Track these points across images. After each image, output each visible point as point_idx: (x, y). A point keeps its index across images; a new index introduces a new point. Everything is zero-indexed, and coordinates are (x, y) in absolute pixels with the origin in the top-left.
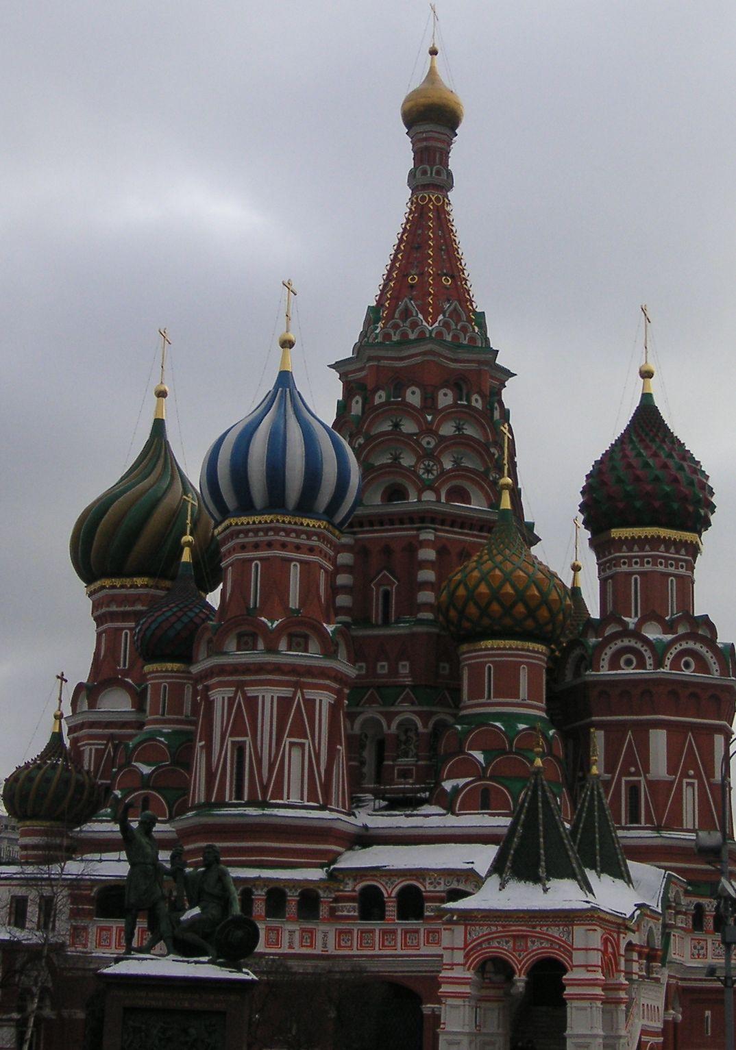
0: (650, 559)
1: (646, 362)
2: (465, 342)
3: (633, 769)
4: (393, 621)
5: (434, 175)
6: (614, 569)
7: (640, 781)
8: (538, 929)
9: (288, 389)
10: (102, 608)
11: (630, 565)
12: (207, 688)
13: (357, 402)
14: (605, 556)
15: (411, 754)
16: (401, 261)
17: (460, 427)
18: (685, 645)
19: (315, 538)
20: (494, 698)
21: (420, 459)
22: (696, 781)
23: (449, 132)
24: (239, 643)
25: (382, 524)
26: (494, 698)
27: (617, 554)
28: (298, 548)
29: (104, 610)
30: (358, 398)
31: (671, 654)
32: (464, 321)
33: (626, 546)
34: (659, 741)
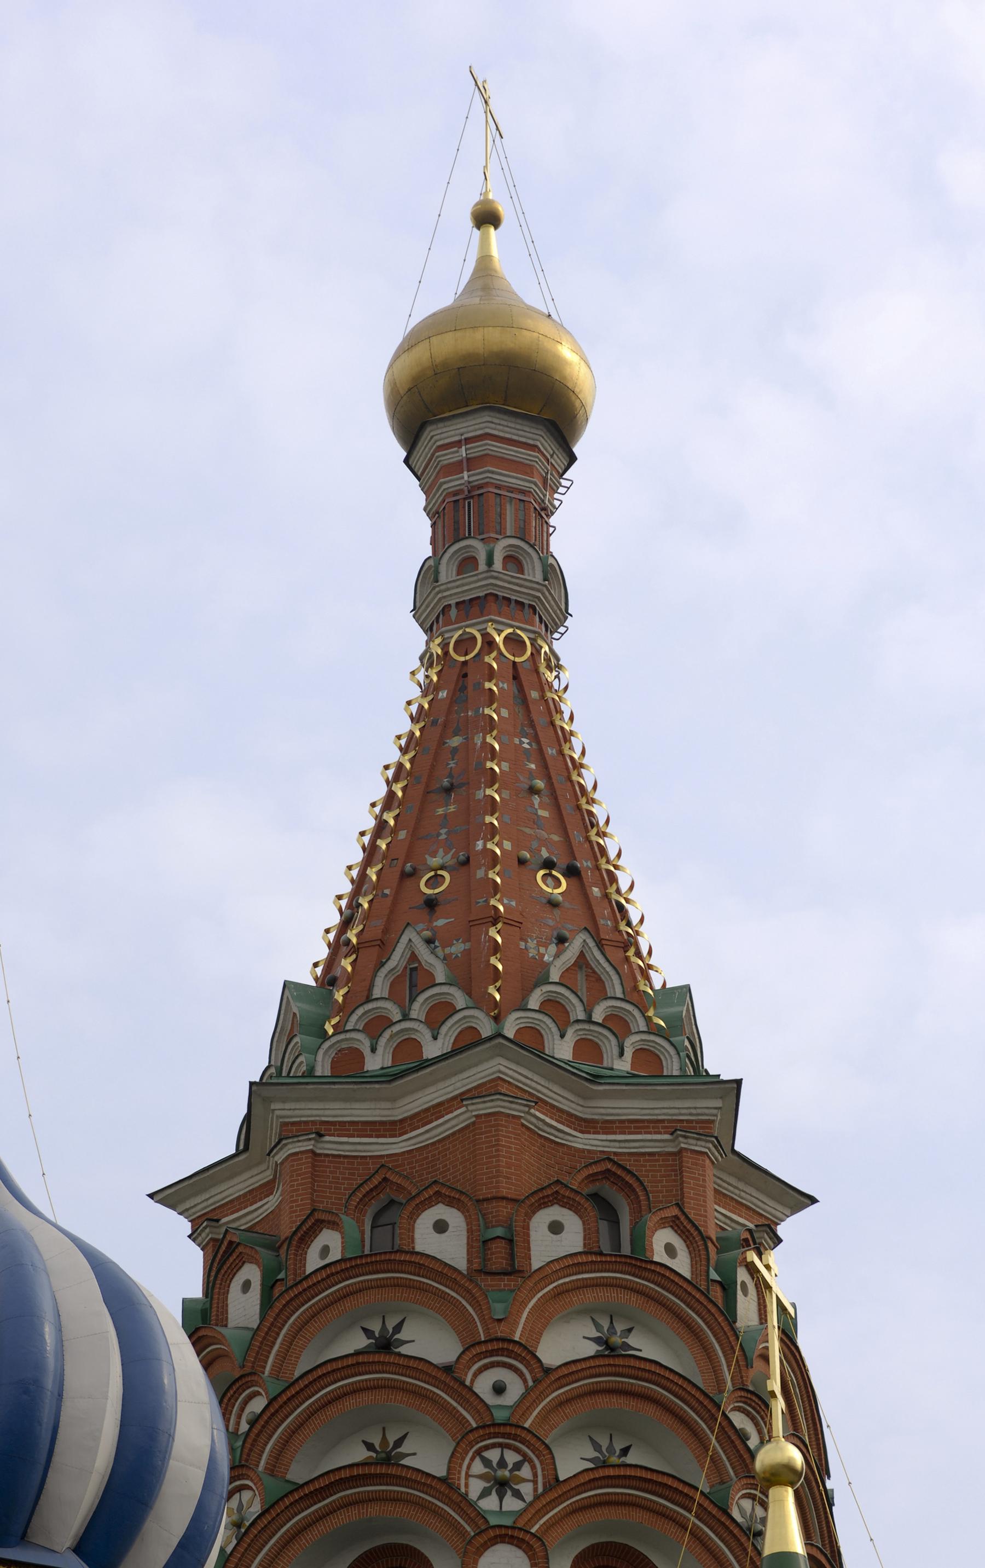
2: (624, 1065)
5: (498, 565)
13: (246, 1286)
16: (394, 831)
17: (616, 1340)
23: (547, 444)
30: (251, 1273)
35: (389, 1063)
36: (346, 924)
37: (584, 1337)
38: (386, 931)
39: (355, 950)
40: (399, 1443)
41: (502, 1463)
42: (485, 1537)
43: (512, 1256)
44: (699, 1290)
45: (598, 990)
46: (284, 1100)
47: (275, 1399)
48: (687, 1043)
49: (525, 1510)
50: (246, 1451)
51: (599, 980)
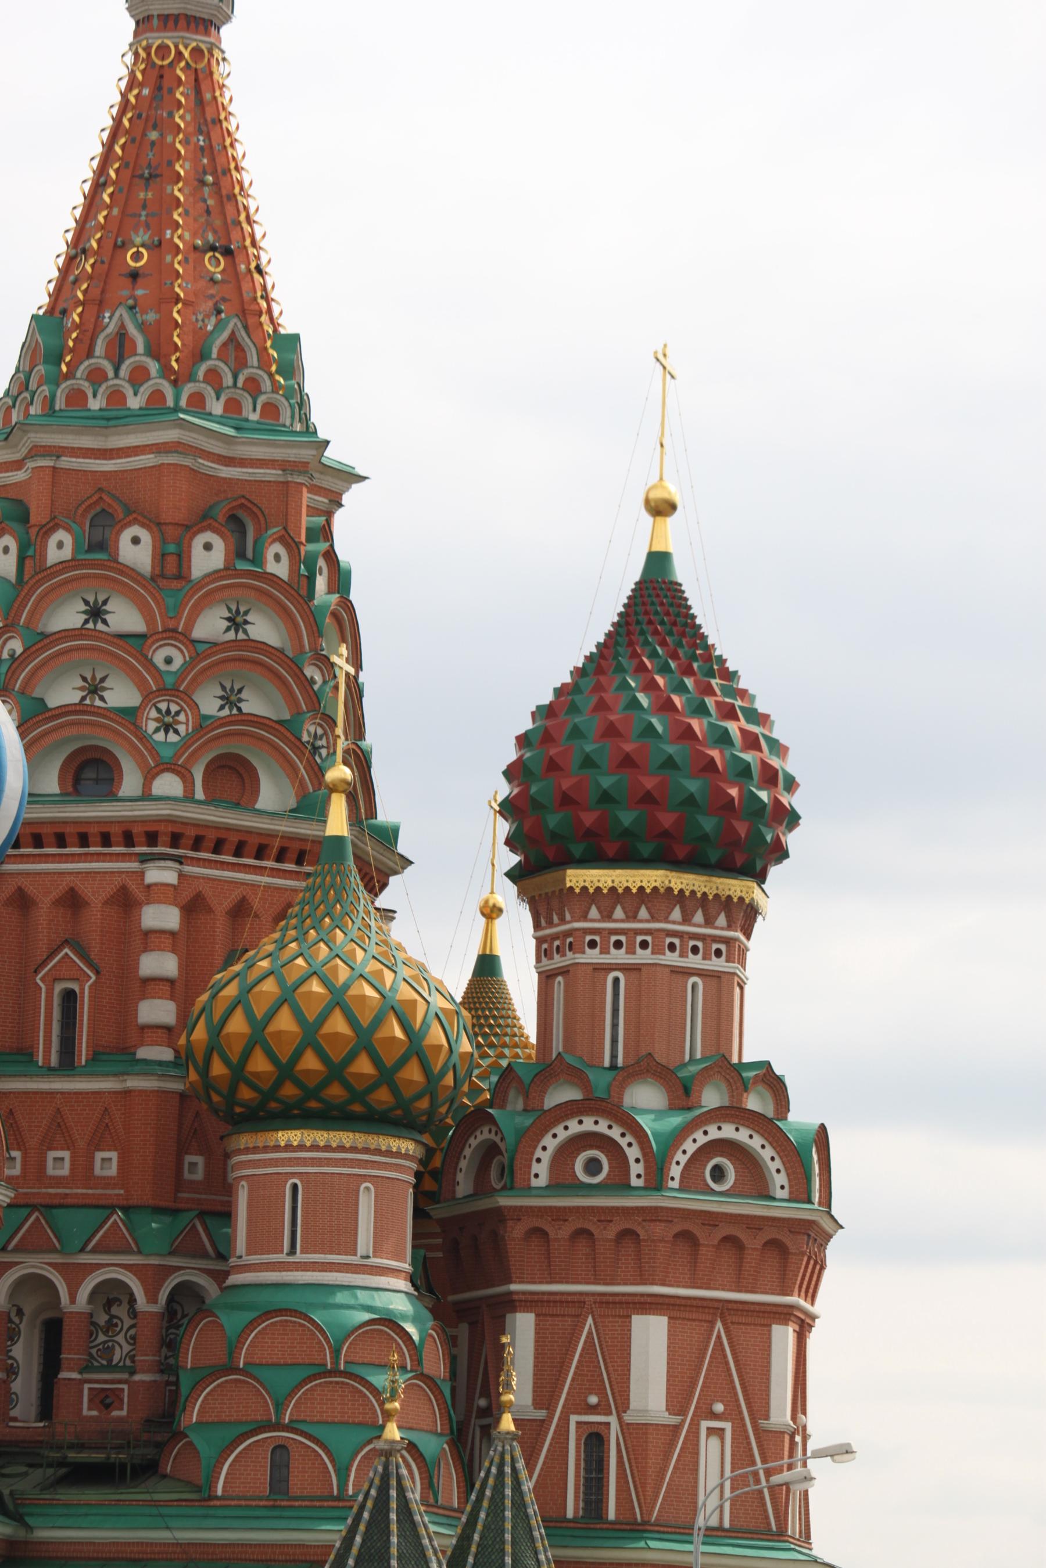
0: (649, 939)
1: (661, 479)
2: (254, 417)
3: (593, 1400)
6: (569, 954)
7: (608, 1424)
11: (605, 951)
14: (550, 924)
15: (116, 1358)
16: (109, 207)
17: (239, 619)
18: (714, 1134)
20: (302, 1252)
21: (148, 697)
22: (727, 1426)
25: (61, 841)
26: (302, 1252)
31: (684, 1152)
32: (253, 367)
33: (598, 908)
35: (104, 405)
36: (70, 260)
37: (221, 618)
38: (103, 292)
39: (83, 304)
40: (103, 680)
41: (168, 712)
42: (158, 769)
43: (179, 566)
44: (293, 589)
45: (241, 363)
46: (36, 432)
47: (28, 648)
48: (296, 386)
49: (180, 741)
50: (8, 677)
51: (243, 350)
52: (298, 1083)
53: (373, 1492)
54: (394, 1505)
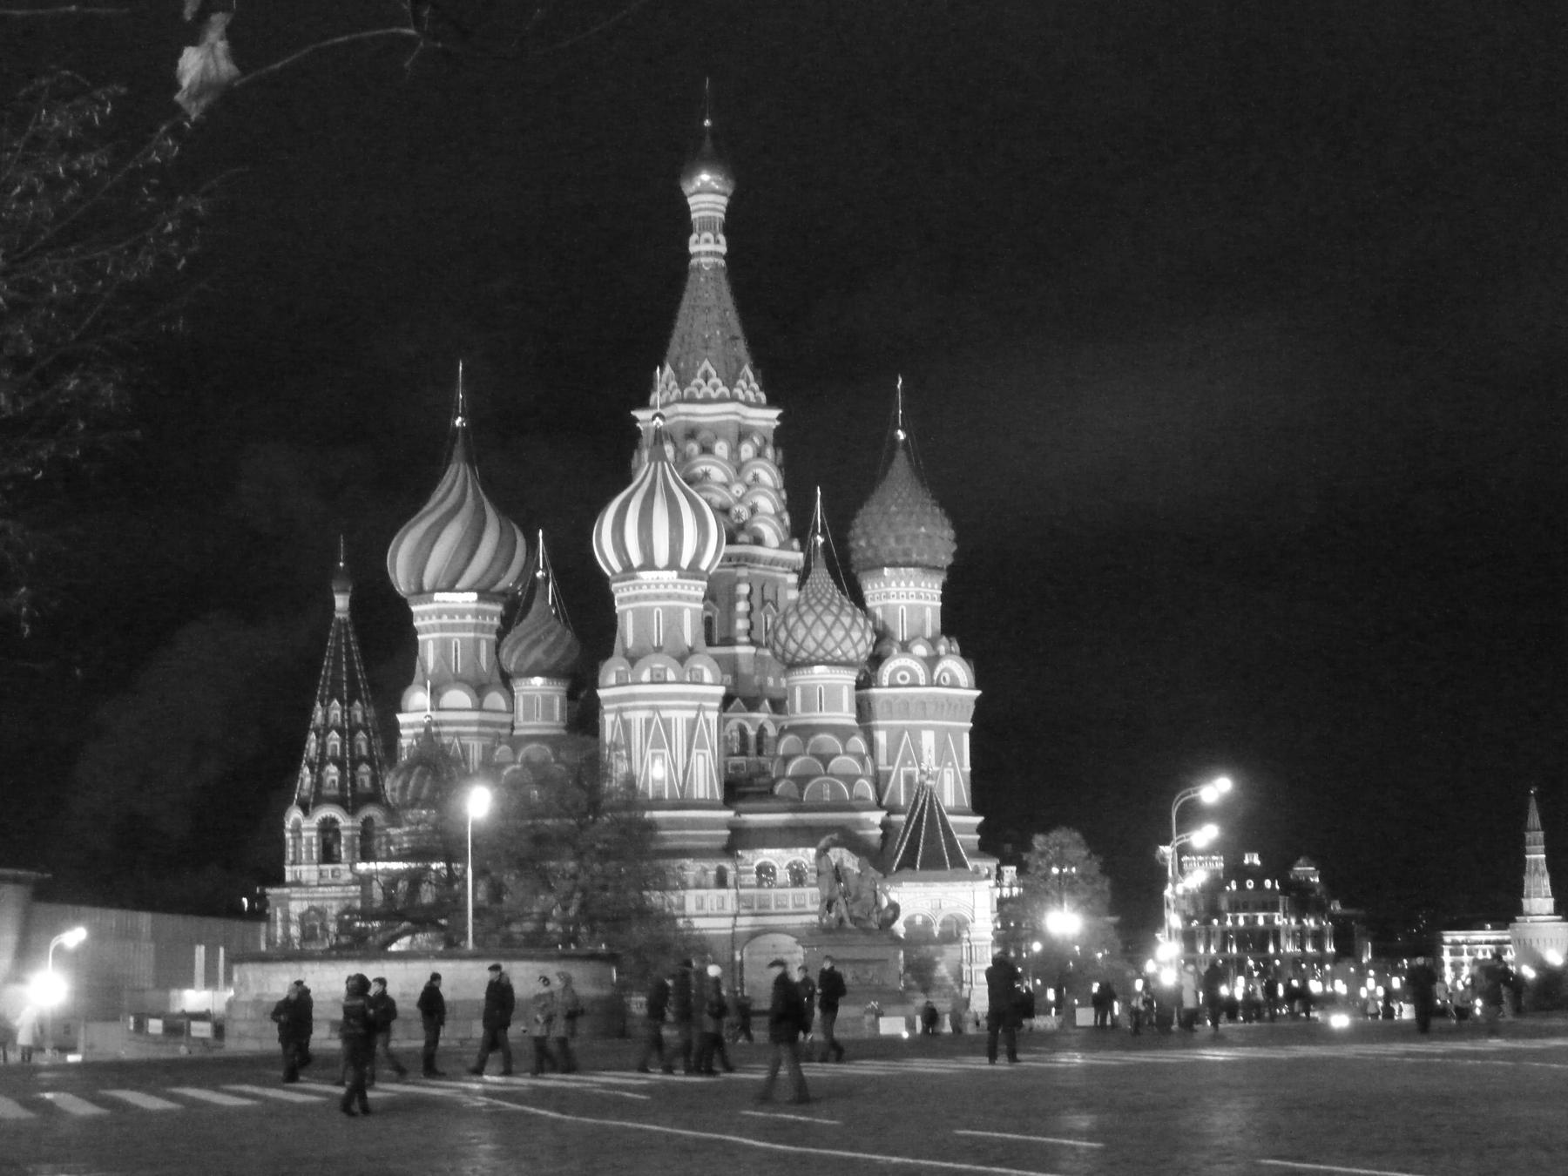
2: (754, 401)
3: (910, 763)
4: (717, 642)
7: (915, 772)
8: (949, 894)
9: (666, 464)
10: (430, 618)
11: (898, 598)
12: (620, 711)
19: (700, 589)
22: (952, 770)
24: (652, 676)
26: (827, 710)
27: (888, 589)
28: (689, 598)
29: (435, 621)
34: (928, 740)
52: (824, 650)
53: (928, 799)
54: (935, 803)
